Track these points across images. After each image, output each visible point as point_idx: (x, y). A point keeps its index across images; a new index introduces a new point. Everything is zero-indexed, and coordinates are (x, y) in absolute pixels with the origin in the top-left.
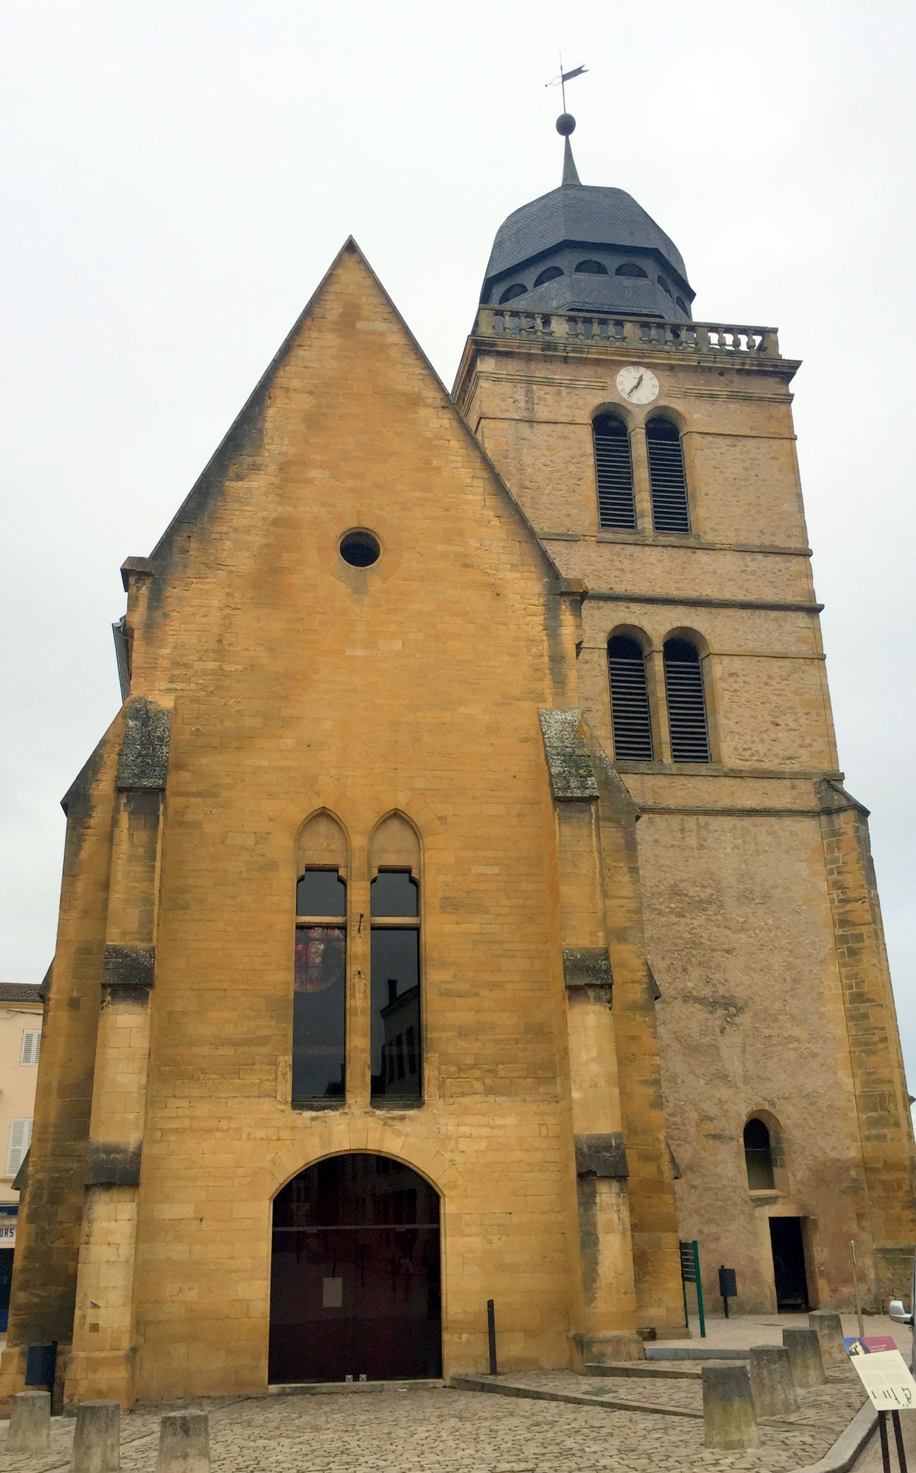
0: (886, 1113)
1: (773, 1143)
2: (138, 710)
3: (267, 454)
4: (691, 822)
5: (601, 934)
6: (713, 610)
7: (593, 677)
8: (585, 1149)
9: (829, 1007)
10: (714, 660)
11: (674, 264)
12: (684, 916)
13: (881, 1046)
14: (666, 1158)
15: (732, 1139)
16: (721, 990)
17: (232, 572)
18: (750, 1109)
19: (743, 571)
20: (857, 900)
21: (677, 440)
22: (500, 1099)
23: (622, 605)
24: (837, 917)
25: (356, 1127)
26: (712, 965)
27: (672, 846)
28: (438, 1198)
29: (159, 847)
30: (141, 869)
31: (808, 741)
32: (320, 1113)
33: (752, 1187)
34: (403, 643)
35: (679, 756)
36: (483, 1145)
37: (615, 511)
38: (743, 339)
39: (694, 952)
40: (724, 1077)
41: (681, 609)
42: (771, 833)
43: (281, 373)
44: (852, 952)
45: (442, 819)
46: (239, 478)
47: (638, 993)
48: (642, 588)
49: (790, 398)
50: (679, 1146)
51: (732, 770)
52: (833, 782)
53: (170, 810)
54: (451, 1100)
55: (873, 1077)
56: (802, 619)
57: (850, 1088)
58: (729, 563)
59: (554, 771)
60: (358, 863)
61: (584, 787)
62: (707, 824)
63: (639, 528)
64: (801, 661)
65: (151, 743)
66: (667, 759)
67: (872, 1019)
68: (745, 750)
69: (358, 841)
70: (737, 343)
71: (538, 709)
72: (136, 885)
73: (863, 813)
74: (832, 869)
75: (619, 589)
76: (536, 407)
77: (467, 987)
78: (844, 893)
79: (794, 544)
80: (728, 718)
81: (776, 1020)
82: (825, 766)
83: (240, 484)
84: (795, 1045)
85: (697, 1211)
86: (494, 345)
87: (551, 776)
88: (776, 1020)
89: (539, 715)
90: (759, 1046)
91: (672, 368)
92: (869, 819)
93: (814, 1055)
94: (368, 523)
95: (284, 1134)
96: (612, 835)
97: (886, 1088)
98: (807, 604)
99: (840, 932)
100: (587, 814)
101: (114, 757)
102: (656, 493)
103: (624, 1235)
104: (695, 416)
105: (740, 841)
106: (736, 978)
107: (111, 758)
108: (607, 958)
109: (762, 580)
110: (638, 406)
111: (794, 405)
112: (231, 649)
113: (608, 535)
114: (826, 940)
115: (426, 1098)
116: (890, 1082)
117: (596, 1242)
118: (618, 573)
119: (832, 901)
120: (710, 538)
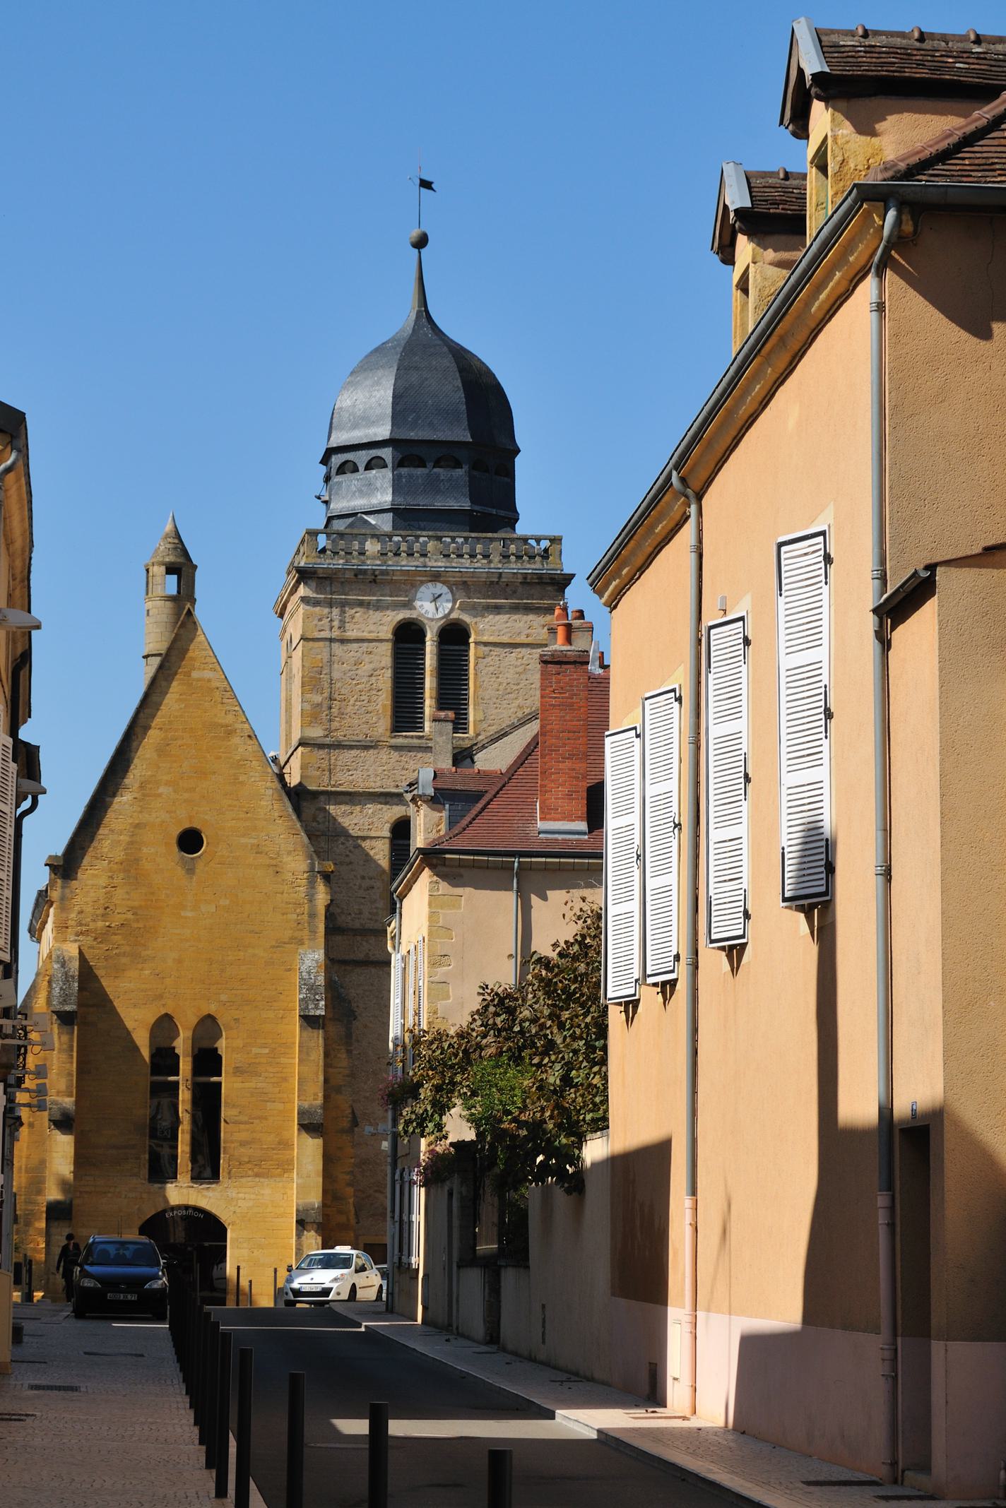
36: (251, 1204)
77: (246, 1119)
94: (196, 825)
95: (145, 1196)
110: (432, 620)
118: (404, 772)
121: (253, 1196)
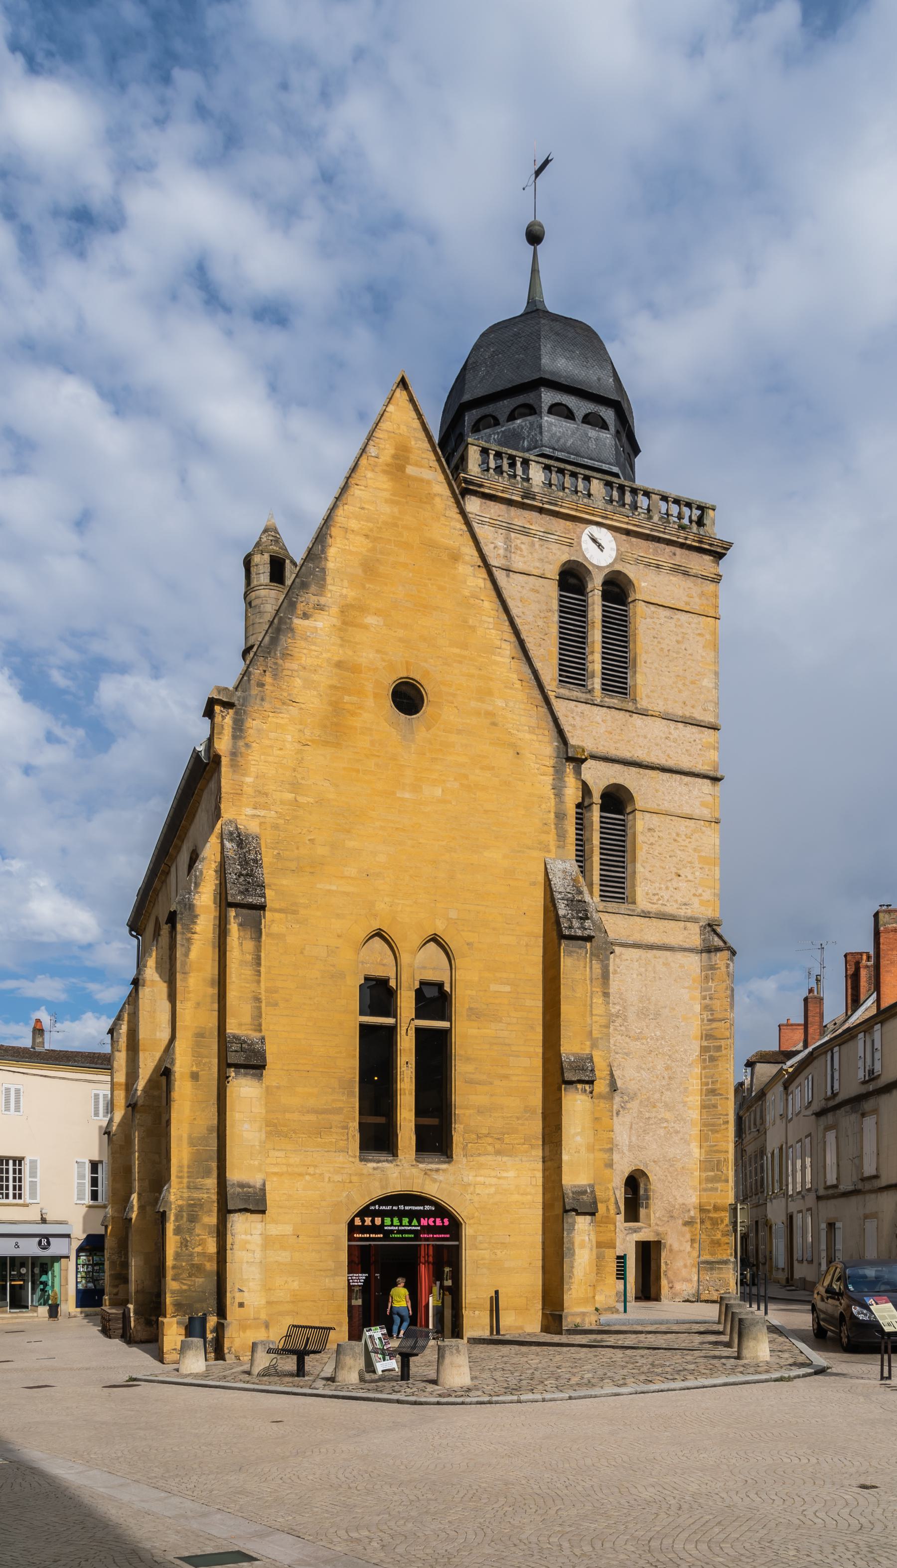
9: (691, 1098)
30: (249, 972)
52: (715, 927)
72: (248, 985)
80: (644, 867)
93: (677, 1132)
105: (643, 970)
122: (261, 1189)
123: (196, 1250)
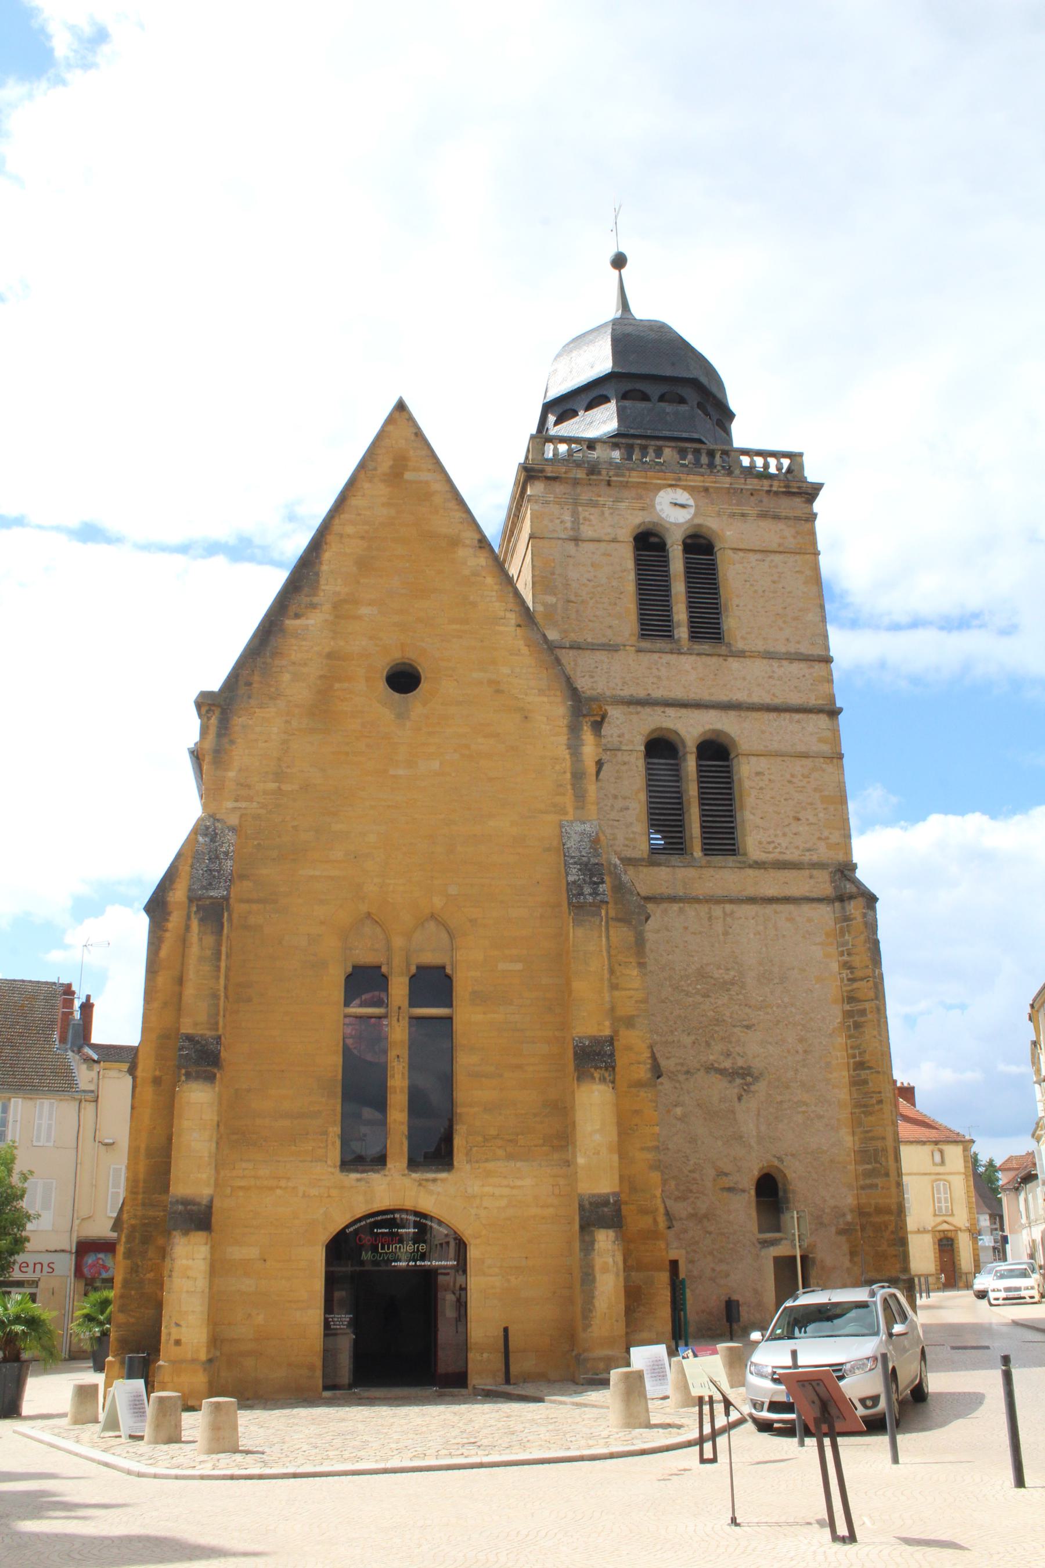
0: (878, 1165)
1: (781, 1194)
2: (207, 828)
3: (322, 594)
4: (717, 911)
5: (607, 1023)
6: (743, 714)
7: (631, 777)
8: (587, 1206)
10: (743, 760)
11: (714, 390)
12: (709, 996)
13: (877, 1107)
14: (662, 1210)
15: (743, 1191)
16: (740, 1062)
17: (290, 701)
18: (761, 1165)
19: (770, 677)
20: (862, 979)
21: (712, 555)
22: (519, 1164)
23: (659, 710)
24: (845, 994)
25: (394, 1188)
26: (734, 1040)
27: (700, 933)
28: (465, 1245)
29: (224, 949)
31: (826, 833)
32: (364, 1175)
33: (761, 1231)
34: (441, 763)
35: (707, 851)
36: (503, 1203)
37: (654, 623)
38: (772, 462)
39: (717, 1028)
40: (739, 1138)
41: (712, 713)
42: (790, 919)
43: (336, 521)
44: (857, 1026)
45: (473, 921)
46: (297, 616)
47: (643, 1072)
48: (678, 693)
49: (814, 516)
50: (698, 1198)
51: (756, 862)
53: (235, 916)
54: (477, 1165)
55: (870, 1135)
56: (823, 720)
57: (850, 1144)
58: (758, 668)
59: (571, 878)
60: (398, 961)
61: (595, 893)
62: (732, 913)
63: (676, 637)
64: (822, 760)
65: (217, 857)
66: (698, 853)
67: (871, 1084)
68: (769, 843)
69: (398, 942)
70: (766, 466)
71: (561, 821)
73: (871, 900)
74: (843, 951)
75: (657, 694)
76: (581, 527)
78: (852, 973)
79: (817, 651)
81: (788, 1087)
82: (841, 857)
83: (298, 622)
84: (804, 1109)
85: (711, 1253)
86: (542, 471)
87: (568, 884)
88: (788, 1087)
89: (561, 826)
90: (771, 1110)
91: (706, 490)
92: (878, 905)
94: (412, 655)
96: (621, 934)
97: (879, 1144)
98: (827, 708)
99: (847, 1007)
100: (599, 918)
101: (188, 868)
102: (691, 606)
103: (617, 1275)
104: (728, 533)
106: (754, 1049)
107: (185, 869)
108: (612, 1044)
109: (788, 683)
110: (676, 524)
111: (818, 523)
112: (289, 770)
113: (646, 644)
114: (834, 1014)
115: (455, 1163)
116: (884, 1138)
117: (594, 1280)
118: (655, 680)
119: (842, 980)
120: (740, 645)
121: (506, 1191)
122: (206, 1206)
123: (148, 1276)
